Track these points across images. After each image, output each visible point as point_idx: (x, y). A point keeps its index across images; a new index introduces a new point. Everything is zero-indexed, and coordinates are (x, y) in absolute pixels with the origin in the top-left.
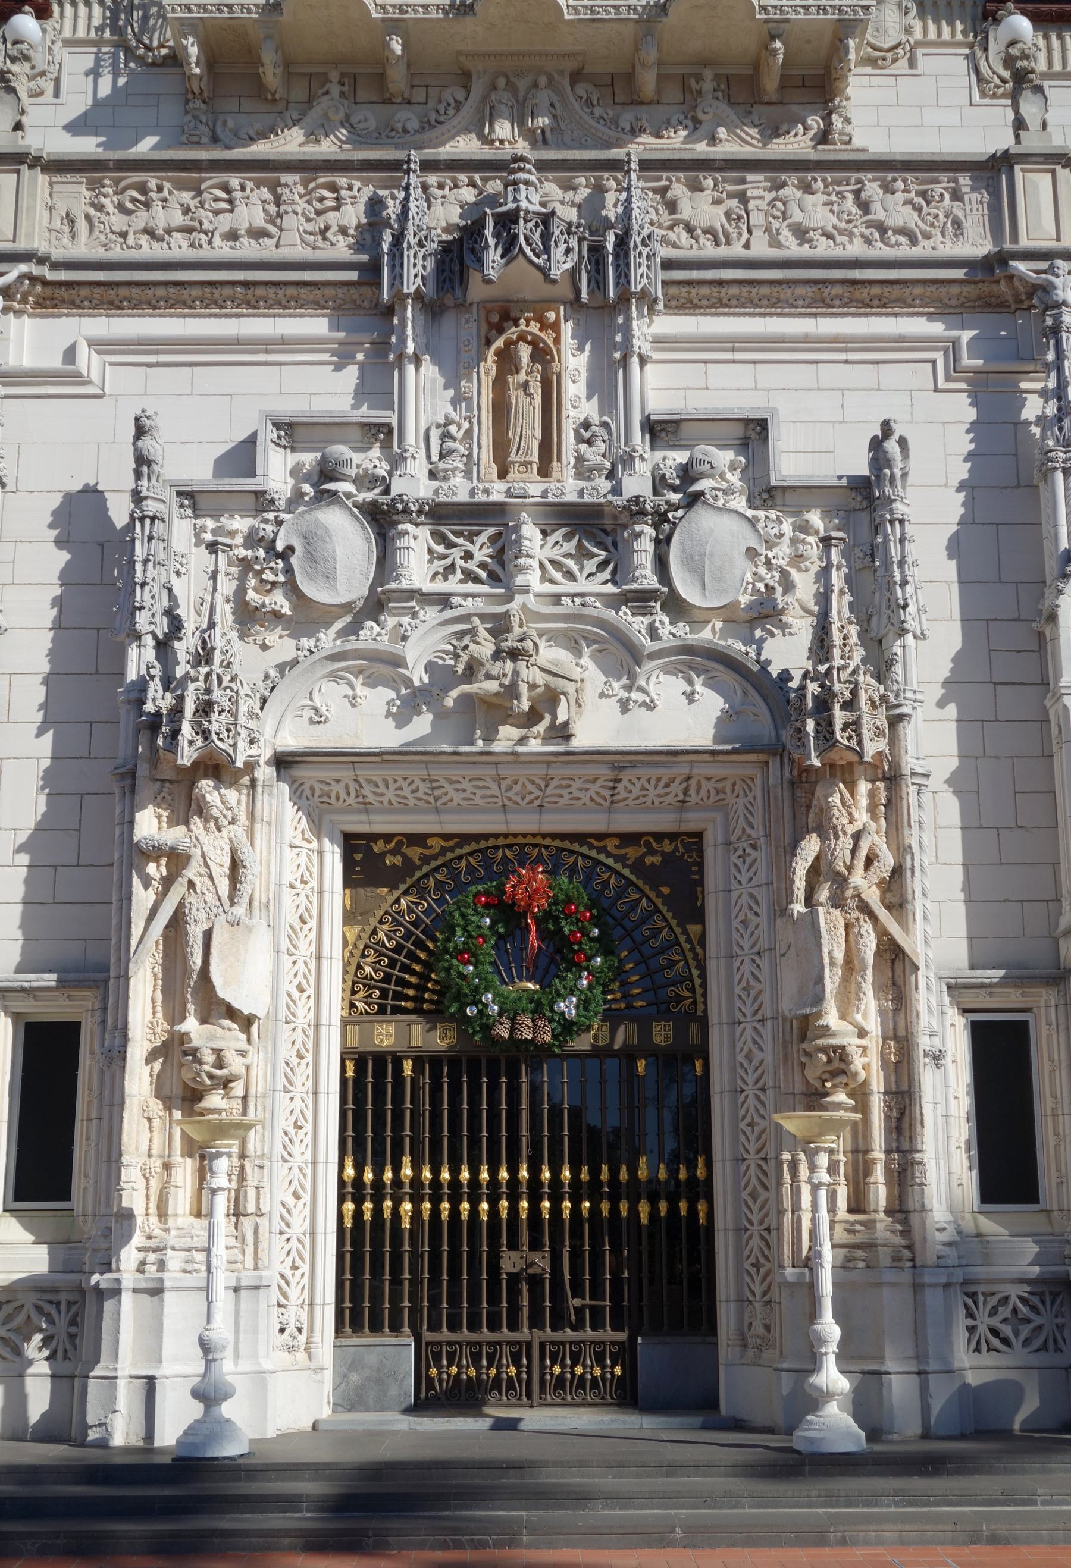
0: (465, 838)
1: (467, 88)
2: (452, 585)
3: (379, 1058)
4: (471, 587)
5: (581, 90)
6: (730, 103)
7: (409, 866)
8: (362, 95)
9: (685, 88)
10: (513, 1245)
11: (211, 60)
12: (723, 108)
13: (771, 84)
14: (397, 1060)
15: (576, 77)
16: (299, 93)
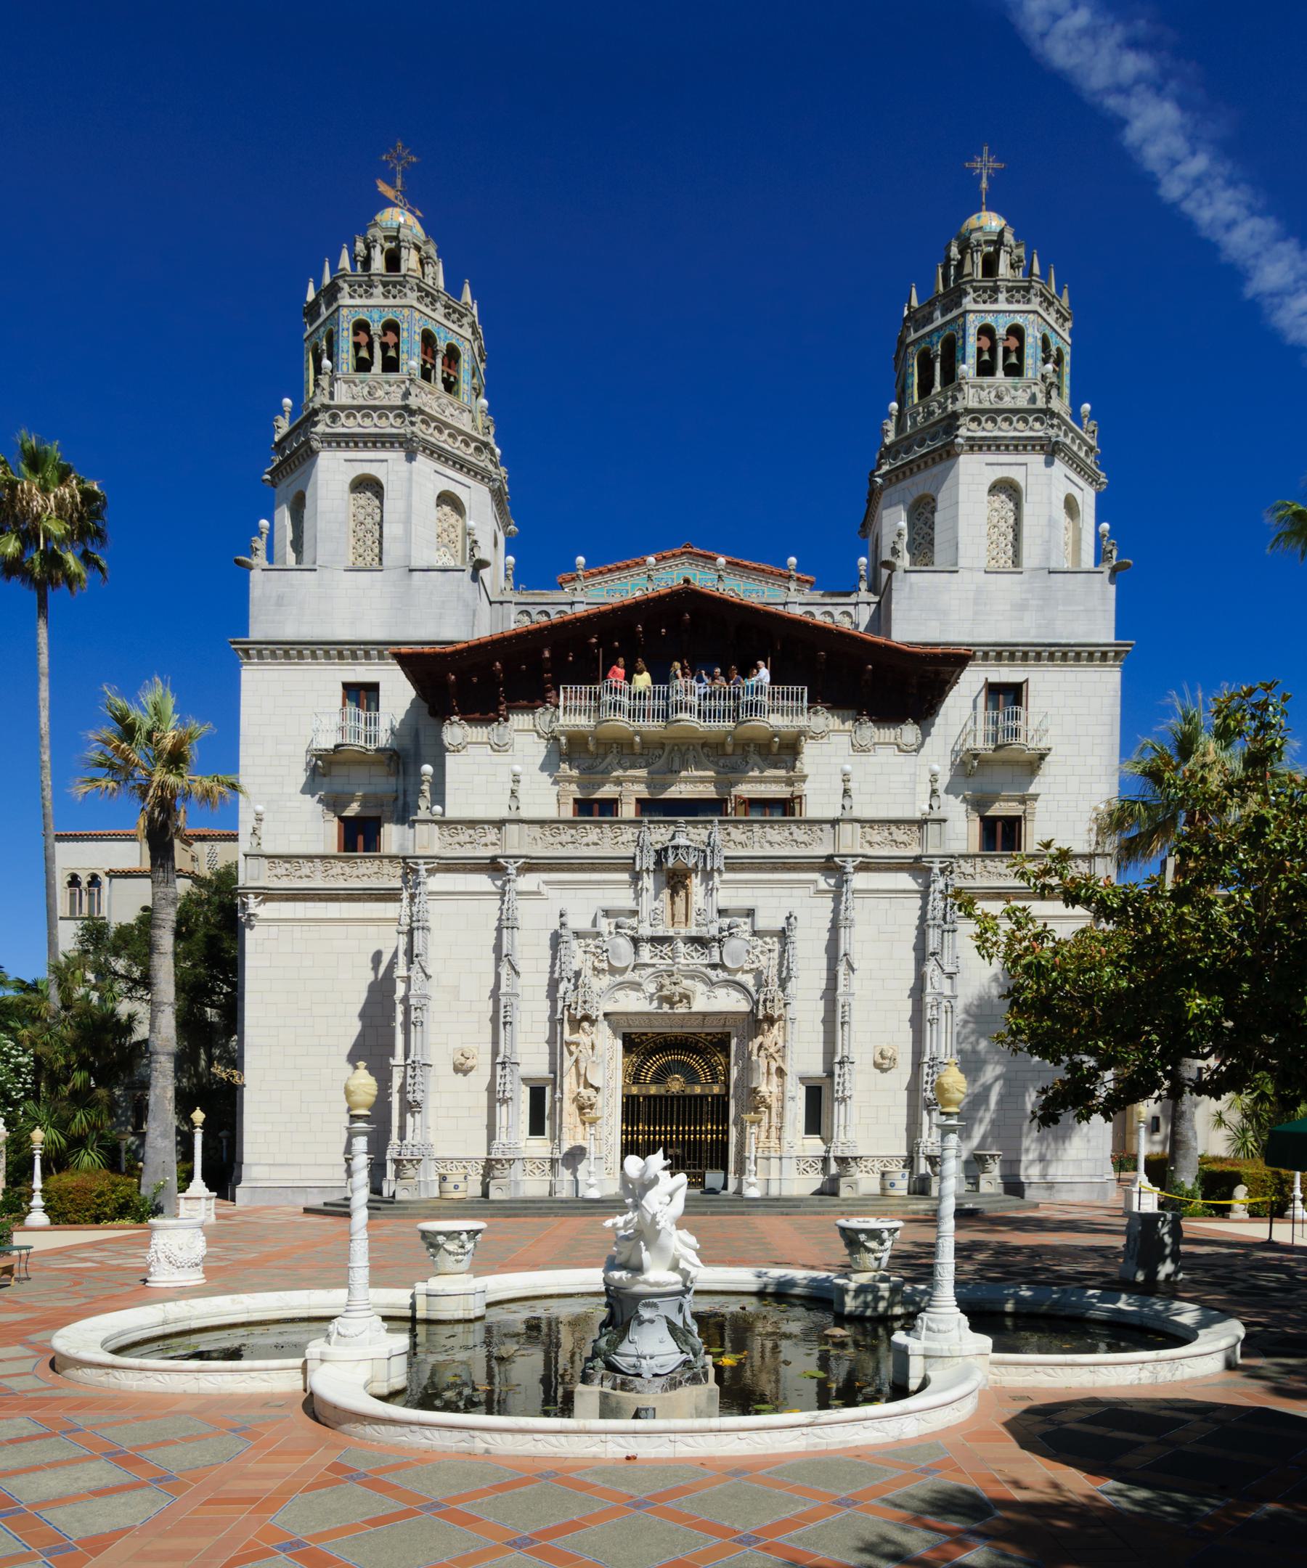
0: (659, 1034)
1: (663, 749)
2: (654, 961)
3: (633, 1096)
4: (662, 961)
5: (705, 750)
6: (760, 754)
7: (642, 1042)
8: (625, 751)
9: (744, 749)
10: (671, 1147)
11: (569, 740)
12: (757, 758)
13: (775, 748)
14: (638, 1097)
15: (704, 745)
16: (601, 751)
